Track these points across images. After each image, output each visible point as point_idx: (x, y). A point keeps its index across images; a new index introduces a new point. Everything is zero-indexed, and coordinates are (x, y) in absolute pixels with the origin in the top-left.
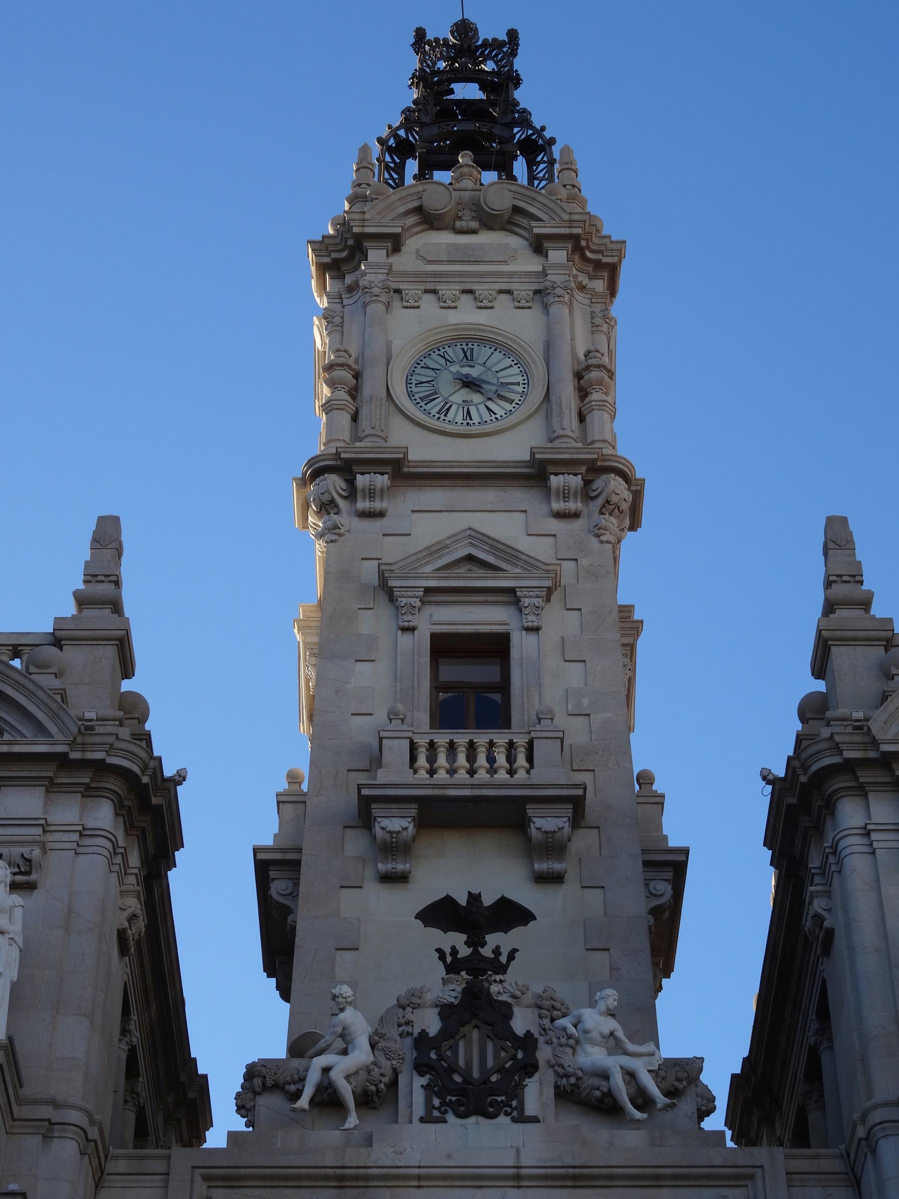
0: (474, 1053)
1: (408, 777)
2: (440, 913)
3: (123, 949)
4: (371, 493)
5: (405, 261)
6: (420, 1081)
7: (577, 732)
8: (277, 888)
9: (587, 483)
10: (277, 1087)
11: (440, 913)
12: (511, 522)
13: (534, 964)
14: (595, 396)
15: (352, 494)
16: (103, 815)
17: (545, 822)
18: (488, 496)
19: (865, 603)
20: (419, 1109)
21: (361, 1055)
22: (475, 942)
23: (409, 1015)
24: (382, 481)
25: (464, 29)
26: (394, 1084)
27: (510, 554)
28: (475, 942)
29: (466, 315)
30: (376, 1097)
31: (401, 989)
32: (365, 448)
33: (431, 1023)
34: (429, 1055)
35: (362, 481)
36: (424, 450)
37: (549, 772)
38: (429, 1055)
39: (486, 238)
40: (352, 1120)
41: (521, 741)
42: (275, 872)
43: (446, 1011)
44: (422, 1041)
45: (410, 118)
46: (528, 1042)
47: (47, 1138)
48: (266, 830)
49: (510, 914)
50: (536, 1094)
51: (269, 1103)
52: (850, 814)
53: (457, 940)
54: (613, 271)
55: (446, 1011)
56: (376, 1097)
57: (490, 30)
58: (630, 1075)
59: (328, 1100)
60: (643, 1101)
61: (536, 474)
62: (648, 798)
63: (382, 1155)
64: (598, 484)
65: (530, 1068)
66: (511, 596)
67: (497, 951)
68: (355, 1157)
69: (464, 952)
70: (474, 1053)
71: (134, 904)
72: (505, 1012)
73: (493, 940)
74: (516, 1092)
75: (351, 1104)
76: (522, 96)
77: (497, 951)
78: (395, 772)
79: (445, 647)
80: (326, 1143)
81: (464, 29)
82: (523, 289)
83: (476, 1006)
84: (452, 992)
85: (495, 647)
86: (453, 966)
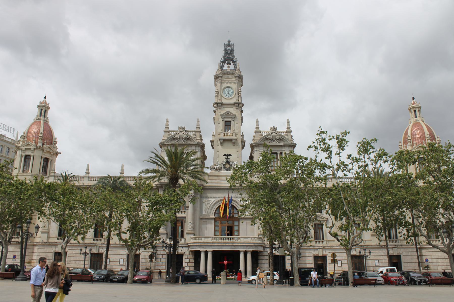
2: (225, 155)
4: (220, 106)
5: (223, 79)
7: (236, 131)
8: (212, 144)
11: (225, 155)
12: (232, 110)
13: (231, 159)
14: (240, 95)
15: (218, 106)
16: (200, 148)
17: (234, 141)
18: (229, 106)
19: (259, 128)
25: (229, 41)
27: (232, 113)
29: (229, 85)
30: (220, 169)
31: (222, 161)
32: (219, 101)
36: (224, 101)
37: (234, 137)
39: (230, 76)
42: (212, 142)
43: (225, 162)
44: (224, 165)
45: (224, 56)
46: (231, 165)
48: (211, 139)
49: (230, 155)
51: (212, 170)
52: (255, 149)
54: (242, 79)
55: (225, 162)
56: (220, 169)
57: (232, 42)
59: (216, 169)
61: (234, 104)
62: (243, 136)
63: (220, 174)
70: (227, 166)
76: (234, 52)
78: (222, 136)
79: (225, 122)
80: (217, 173)
81: (229, 41)
82: (234, 82)
83: (228, 162)
84: (226, 161)
85: (231, 122)
86: (226, 159)
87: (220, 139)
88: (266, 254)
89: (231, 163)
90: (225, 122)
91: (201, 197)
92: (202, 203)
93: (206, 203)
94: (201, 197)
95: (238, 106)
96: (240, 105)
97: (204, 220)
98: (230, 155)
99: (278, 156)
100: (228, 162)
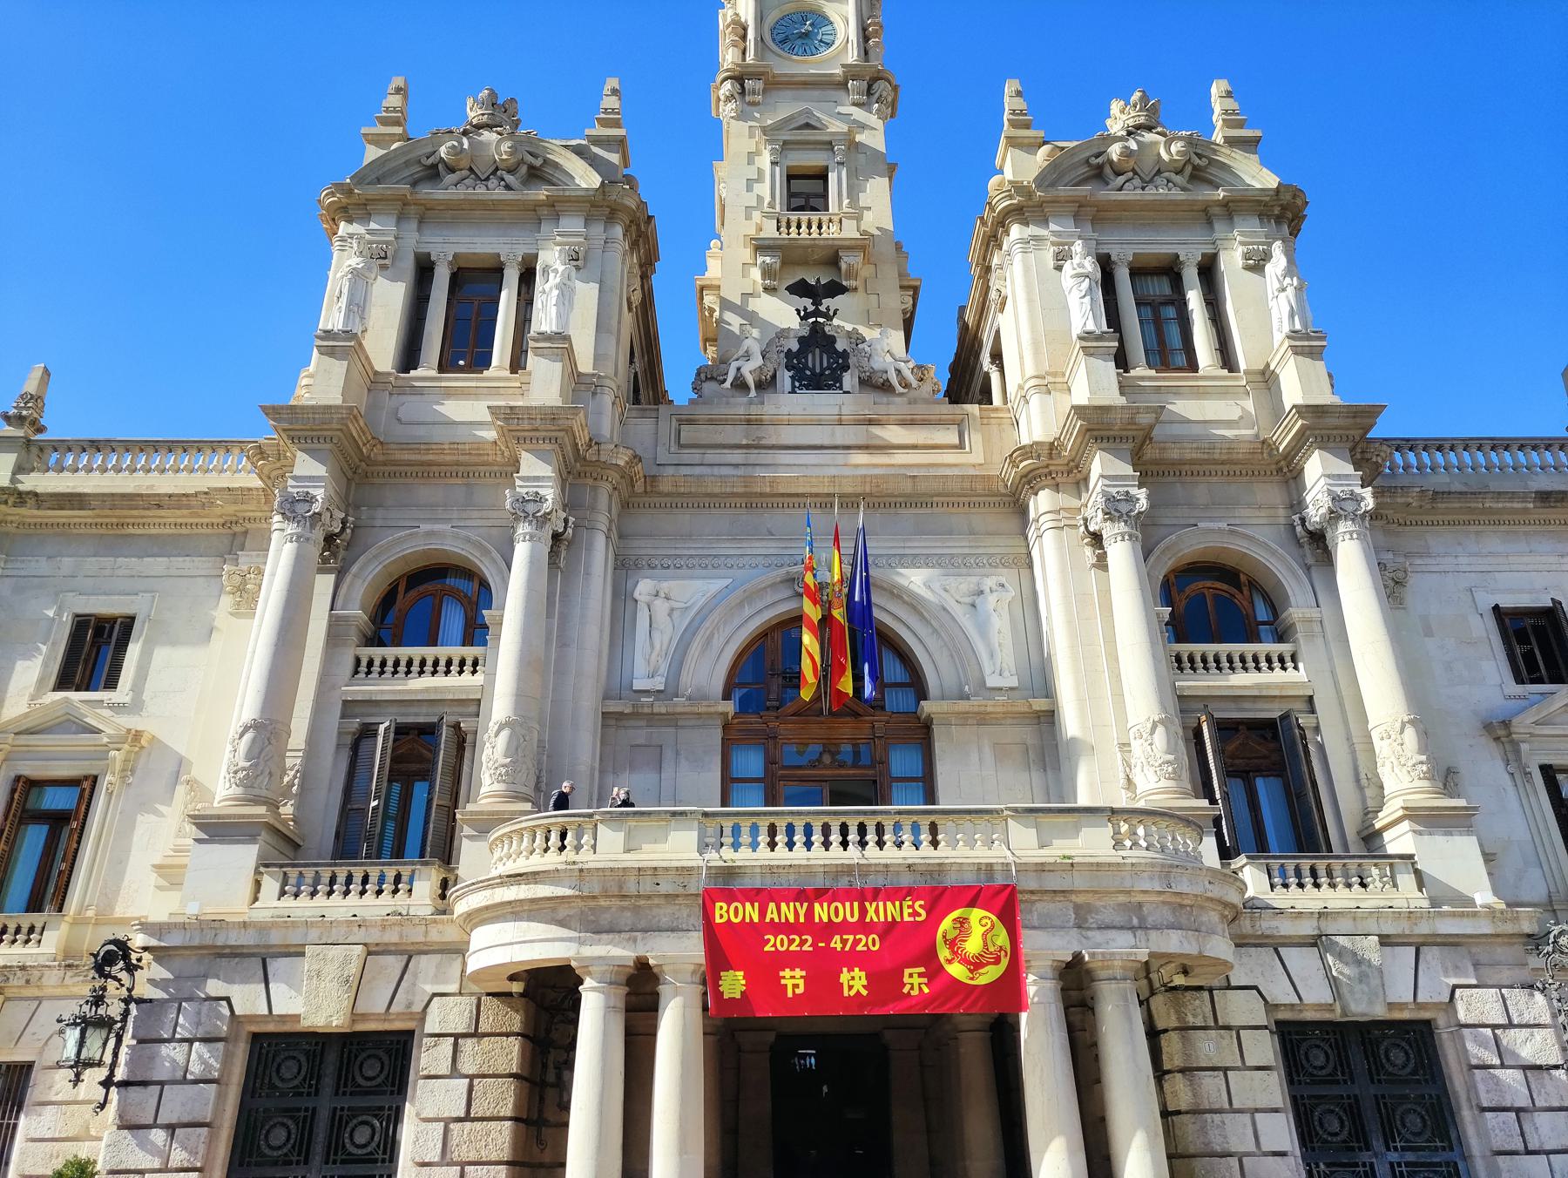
0: (816, 361)
1: (777, 235)
3: (630, 309)
6: (788, 374)
9: (870, 87)
10: (712, 378)
15: (743, 92)
16: (618, 231)
20: (788, 387)
21: (757, 361)
22: (817, 303)
23: (782, 342)
24: (759, 85)
26: (774, 377)
28: (817, 303)
33: (795, 346)
34: (794, 361)
35: (748, 84)
38: (794, 361)
40: (753, 393)
41: (836, 219)
43: (801, 340)
44: (789, 353)
46: (845, 355)
47: (594, 394)
50: (849, 380)
51: (709, 387)
52: (1016, 231)
53: (807, 302)
55: (801, 340)
56: (766, 384)
58: (898, 371)
59: (740, 385)
60: (907, 386)
64: (875, 86)
65: (846, 368)
66: (829, 146)
67: (828, 309)
68: (754, 410)
69: (811, 308)
70: (816, 361)
71: (637, 283)
72: (832, 340)
73: (826, 302)
74: (839, 380)
75: (752, 386)
77: (828, 309)
78: (770, 230)
80: (740, 406)
83: (817, 339)
84: (805, 332)
87: (761, 247)
88: (1241, 1009)
89: (840, 346)
90: (791, 177)
91: (625, 566)
92: (622, 598)
93: (661, 607)
94: (625, 566)
95: (869, 93)
96: (881, 86)
97: (640, 735)
98: (836, 289)
99: (1191, 275)
100: (817, 339)
